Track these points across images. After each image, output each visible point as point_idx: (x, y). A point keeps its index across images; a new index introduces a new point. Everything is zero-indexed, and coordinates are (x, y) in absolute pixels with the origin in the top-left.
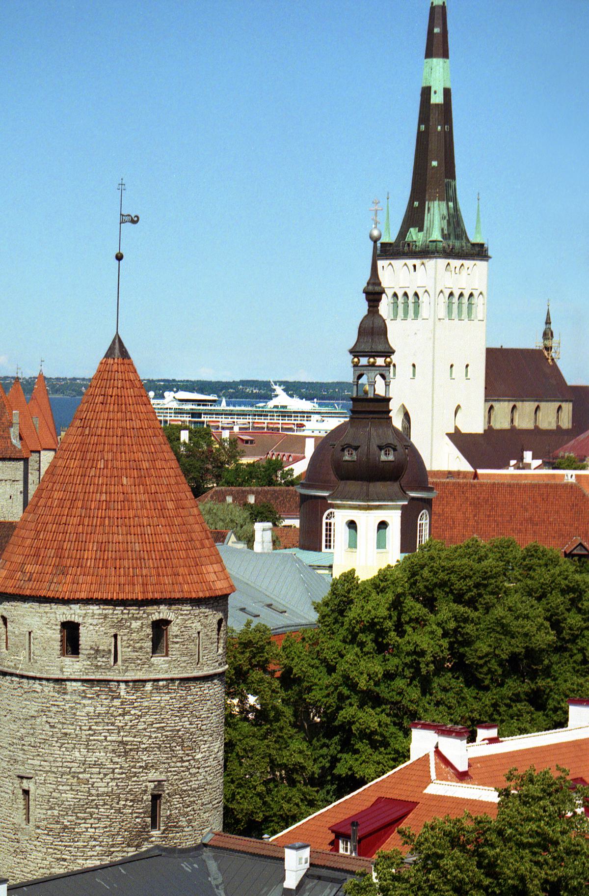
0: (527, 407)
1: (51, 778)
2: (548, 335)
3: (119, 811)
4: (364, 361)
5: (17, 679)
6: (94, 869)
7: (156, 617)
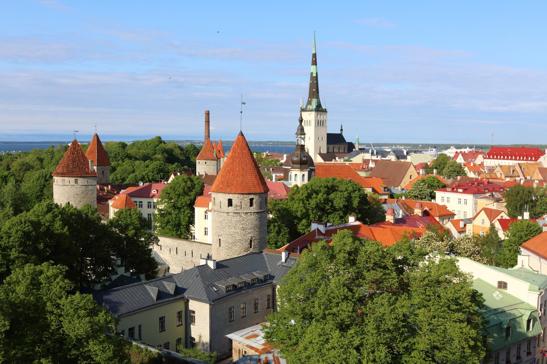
1: (226, 236)
2: (342, 130)
3: (242, 244)
4: (299, 136)
5: (217, 212)
6: (237, 258)
7: (251, 197)
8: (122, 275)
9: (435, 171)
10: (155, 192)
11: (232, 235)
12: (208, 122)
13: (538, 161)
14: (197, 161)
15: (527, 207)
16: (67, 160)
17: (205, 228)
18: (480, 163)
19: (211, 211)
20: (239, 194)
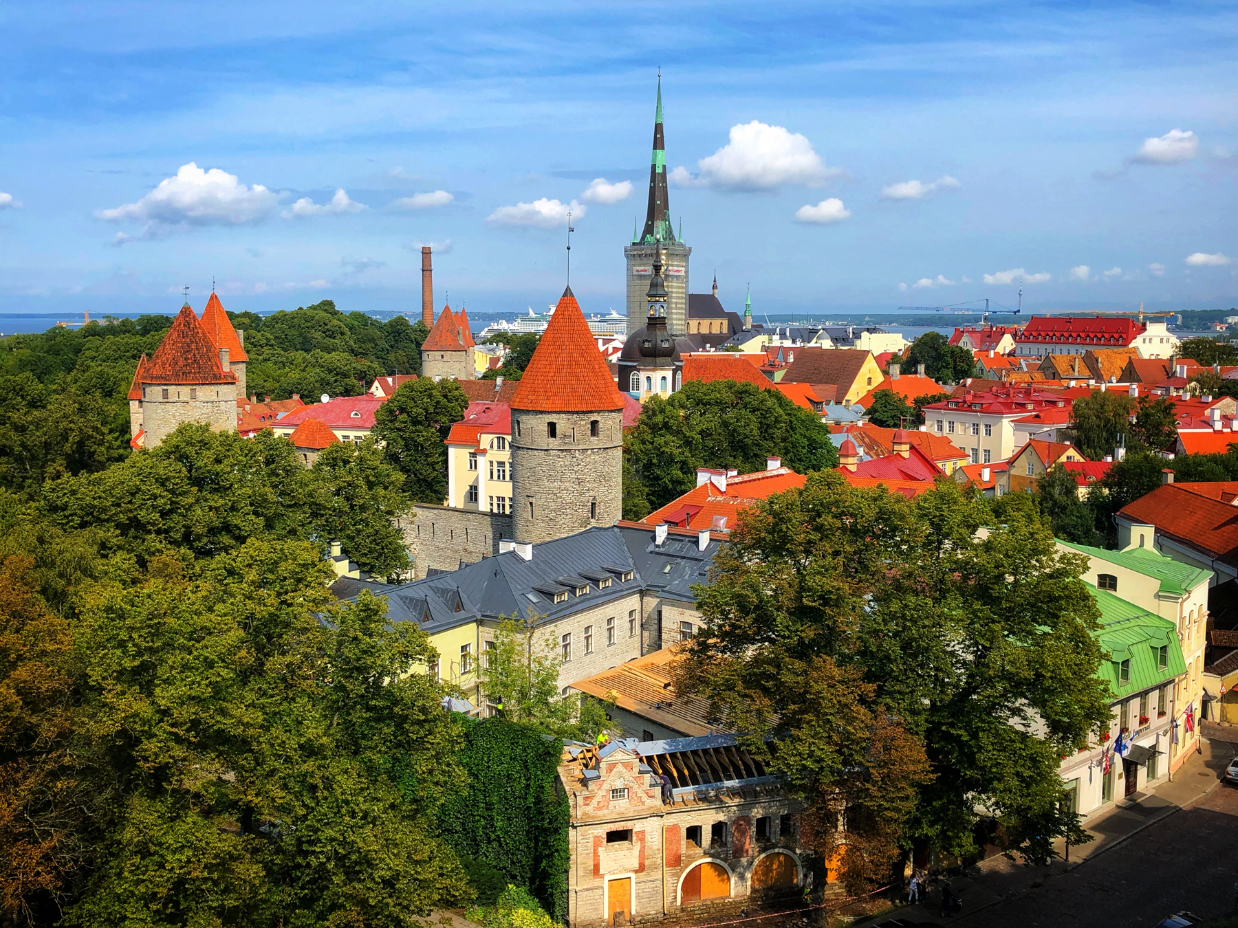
0: (706, 322)
1: (544, 497)
8: (344, 577)
9: (921, 368)
10: (356, 414)
11: (555, 494)
12: (426, 270)
13: (1131, 346)
14: (425, 355)
15: (1121, 438)
16: (171, 349)
17: (471, 487)
18: (1007, 352)
19: (484, 452)
20: (569, 412)
